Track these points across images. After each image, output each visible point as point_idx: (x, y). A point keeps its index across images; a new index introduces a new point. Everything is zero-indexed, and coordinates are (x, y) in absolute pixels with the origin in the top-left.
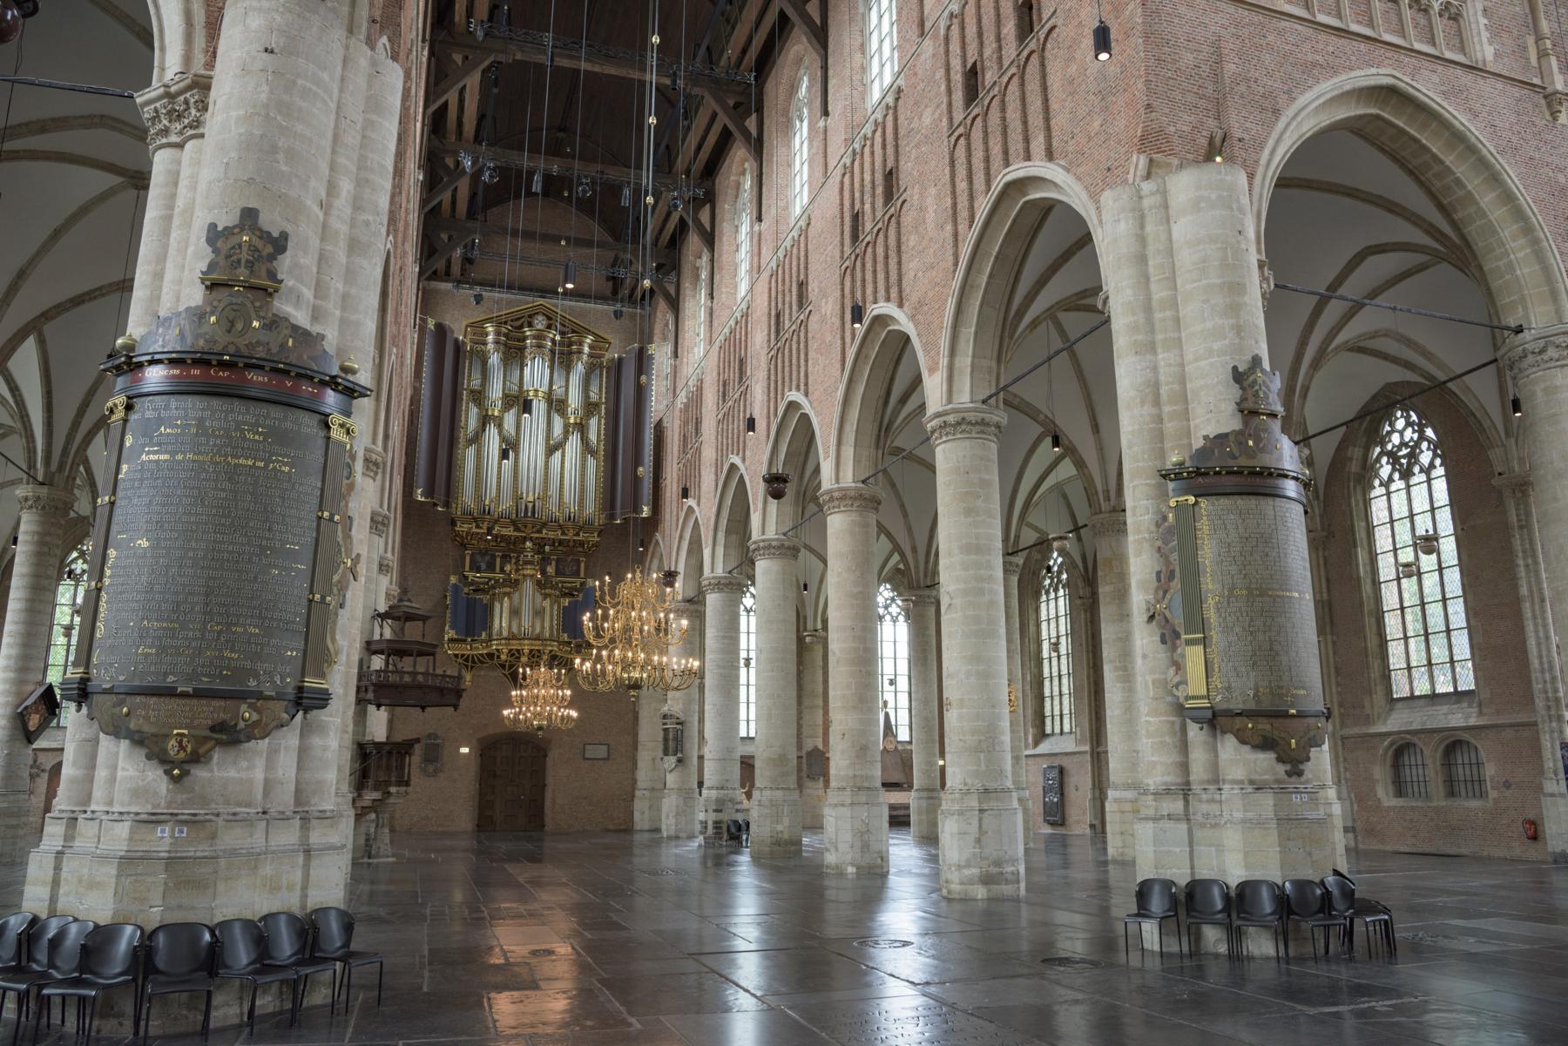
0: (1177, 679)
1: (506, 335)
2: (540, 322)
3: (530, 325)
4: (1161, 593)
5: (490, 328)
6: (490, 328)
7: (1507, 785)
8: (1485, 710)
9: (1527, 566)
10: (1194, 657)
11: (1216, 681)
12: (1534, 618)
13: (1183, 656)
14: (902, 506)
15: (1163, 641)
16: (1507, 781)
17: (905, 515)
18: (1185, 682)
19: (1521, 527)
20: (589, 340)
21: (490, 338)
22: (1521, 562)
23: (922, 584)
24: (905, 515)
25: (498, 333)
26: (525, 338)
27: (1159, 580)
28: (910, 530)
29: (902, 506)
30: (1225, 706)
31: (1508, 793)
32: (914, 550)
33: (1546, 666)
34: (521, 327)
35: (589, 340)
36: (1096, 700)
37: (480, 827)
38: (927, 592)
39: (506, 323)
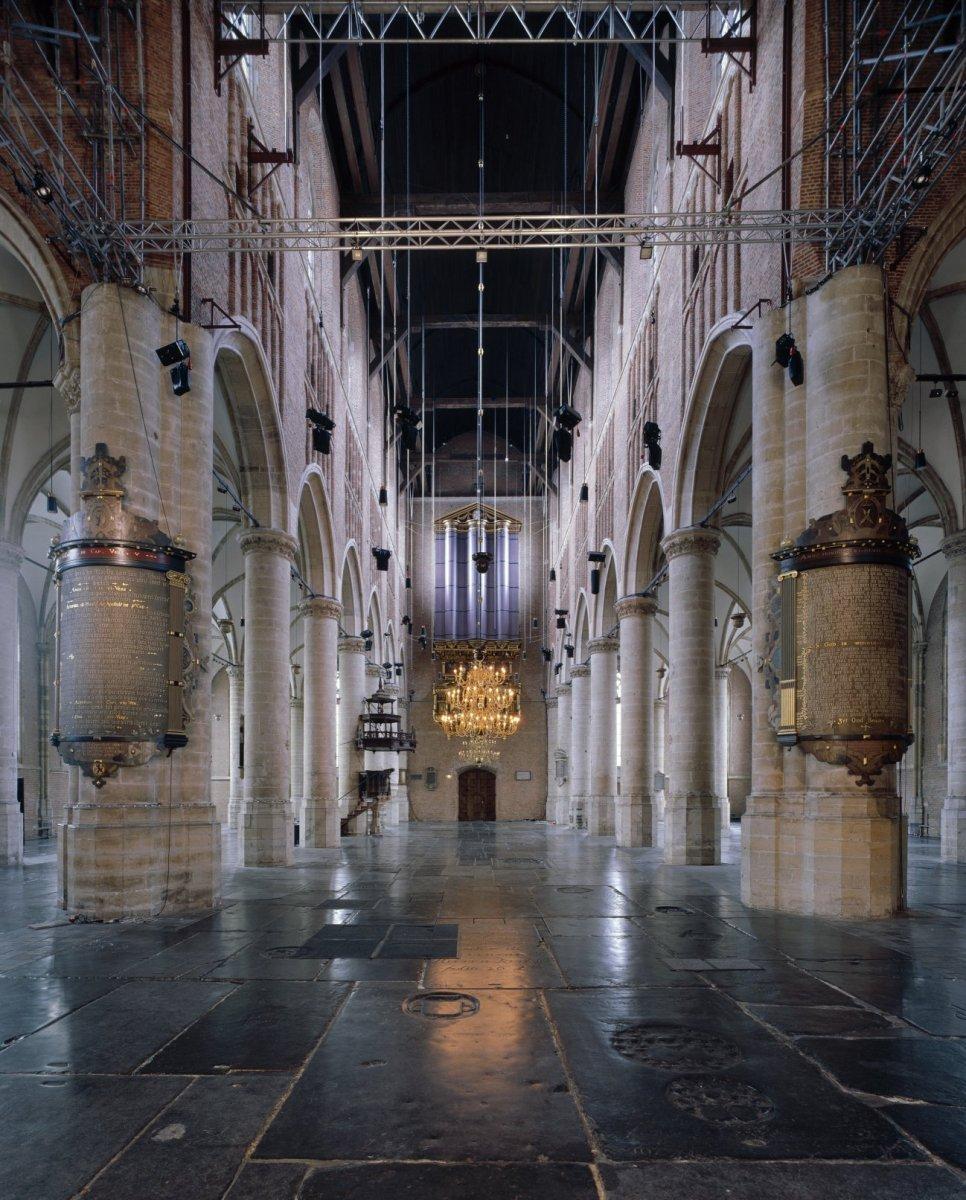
0: (775, 714)
1: (457, 527)
2: (477, 515)
3: (471, 517)
4: (768, 649)
5: (447, 523)
6: (447, 523)
10: (787, 697)
11: (803, 714)
13: (780, 696)
15: (768, 687)
18: (779, 716)
20: (508, 523)
21: (448, 530)
25: (452, 526)
26: (467, 528)
27: (767, 640)
30: (808, 733)
34: (466, 519)
35: (508, 523)
37: (461, 819)
39: (456, 518)
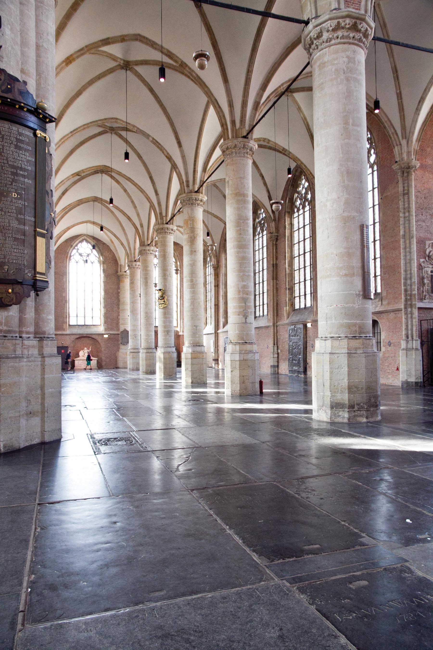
7: (390, 344)
8: (384, 303)
9: (405, 217)
12: (405, 248)
14: (133, 202)
16: (389, 342)
17: (135, 207)
19: (404, 194)
22: (401, 215)
23: (146, 244)
24: (135, 207)
28: (138, 215)
29: (133, 202)
31: (389, 349)
32: (142, 226)
33: (409, 276)
36: (218, 300)
38: (148, 248)
